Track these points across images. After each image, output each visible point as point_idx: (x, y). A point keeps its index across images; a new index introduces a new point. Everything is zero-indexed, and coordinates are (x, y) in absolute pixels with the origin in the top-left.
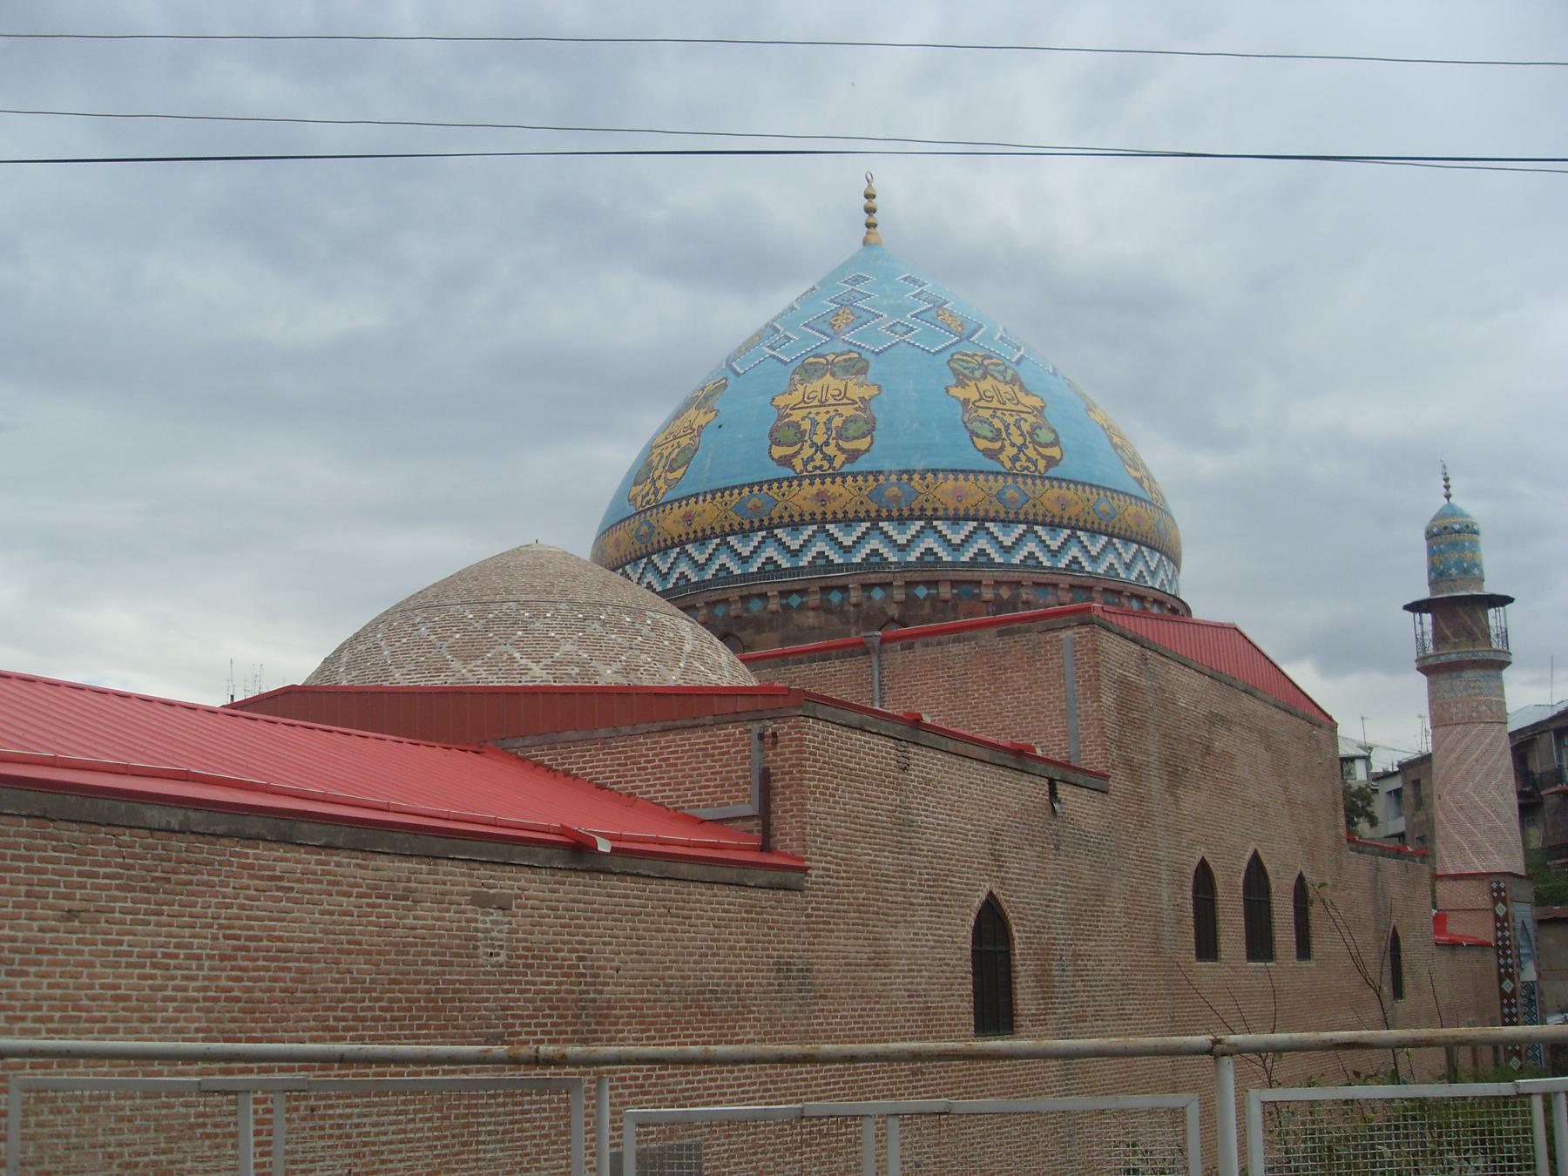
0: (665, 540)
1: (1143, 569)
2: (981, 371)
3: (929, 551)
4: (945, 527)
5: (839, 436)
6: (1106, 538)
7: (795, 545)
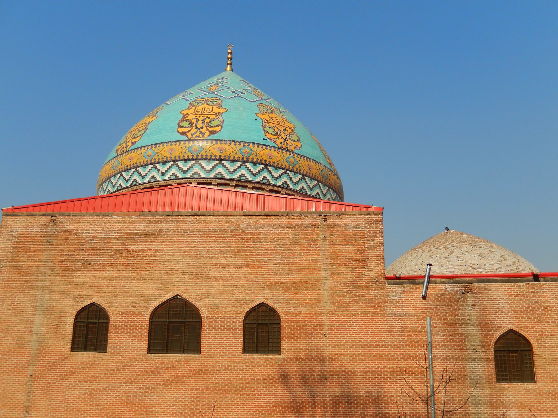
0: (127, 166)
1: (330, 198)
2: (271, 111)
3: (243, 175)
4: (250, 166)
5: (208, 125)
6: (316, 182)
7: (185, 169)
